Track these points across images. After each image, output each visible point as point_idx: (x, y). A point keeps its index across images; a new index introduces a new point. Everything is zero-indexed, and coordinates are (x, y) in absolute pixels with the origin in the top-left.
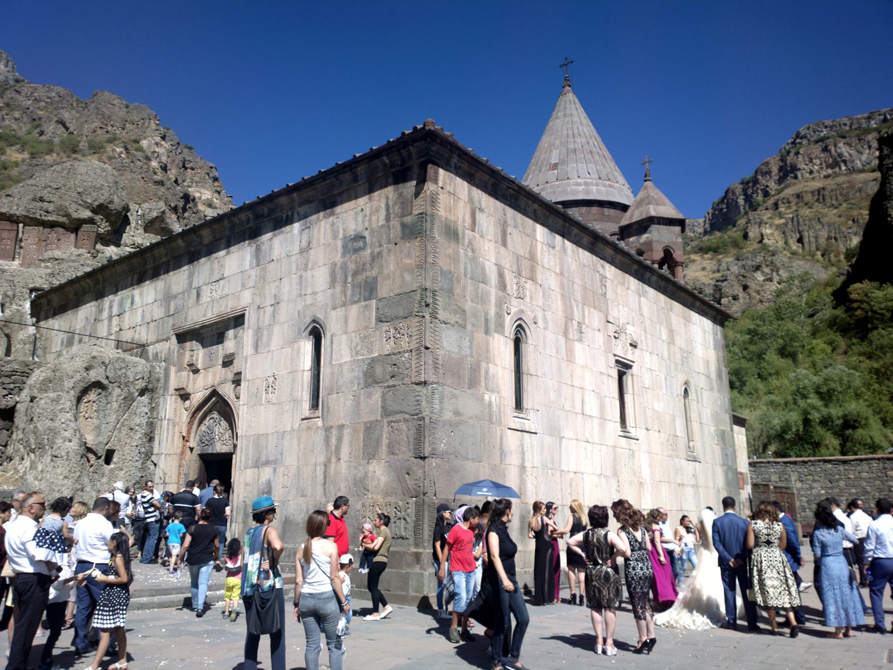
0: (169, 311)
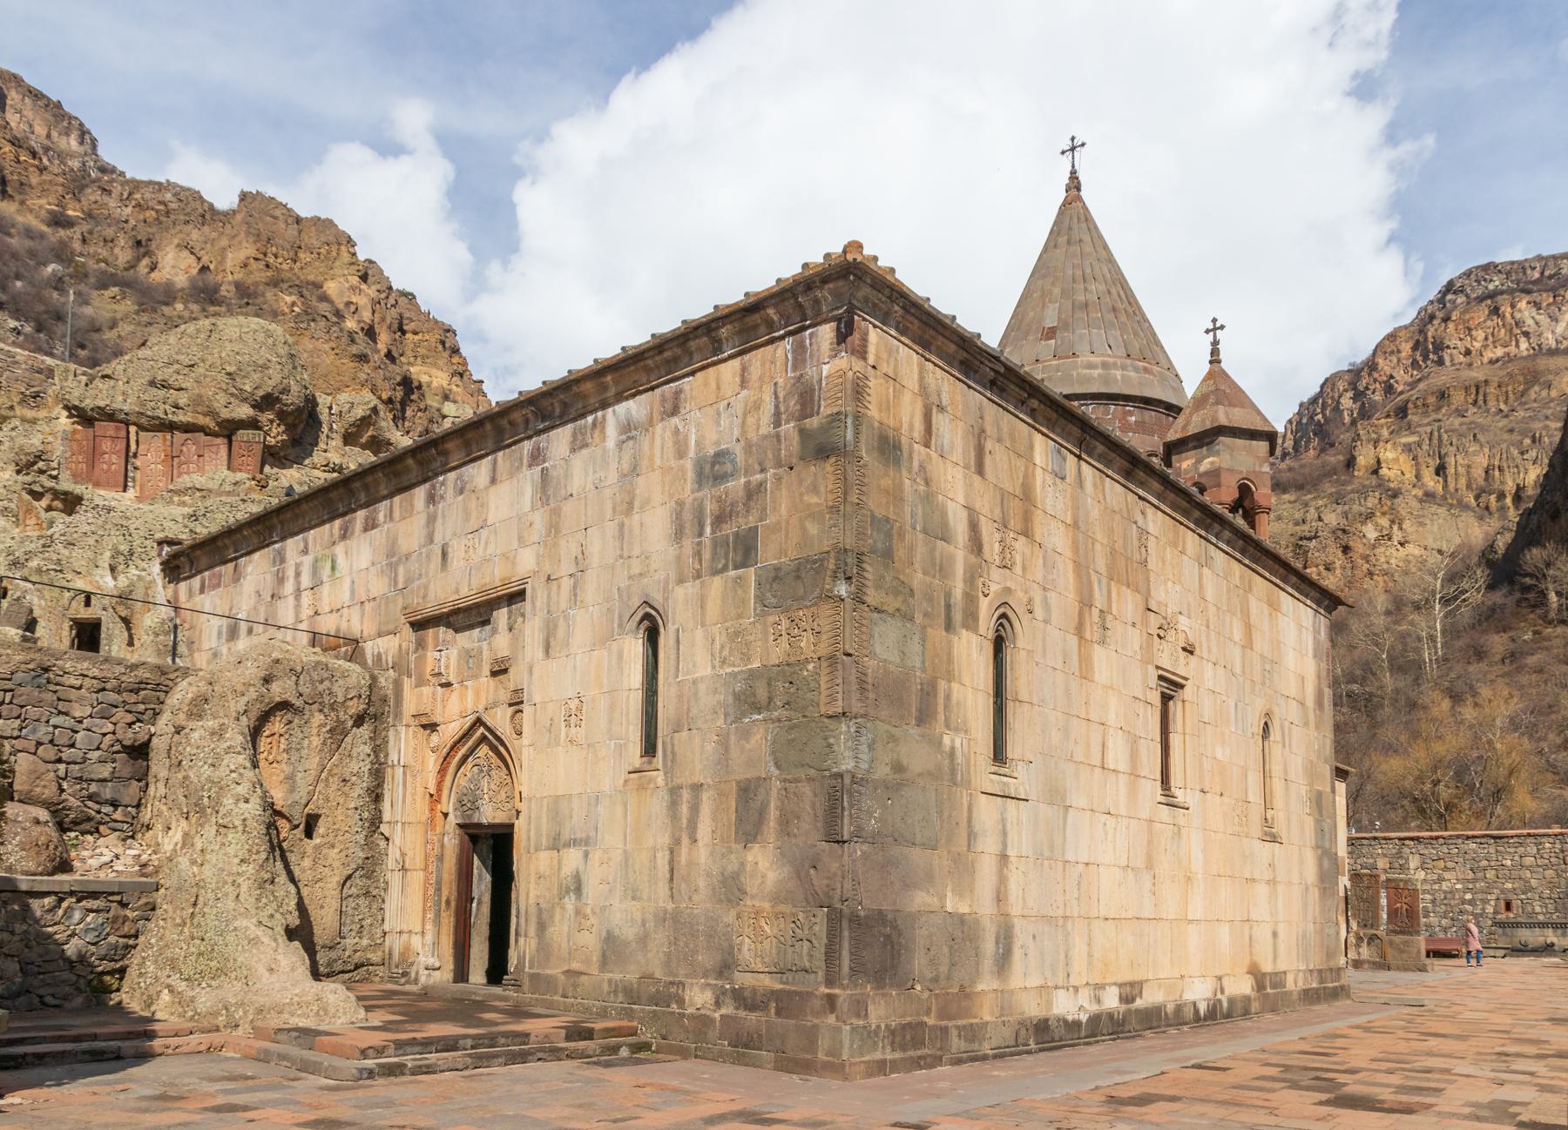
0: (396, 584)
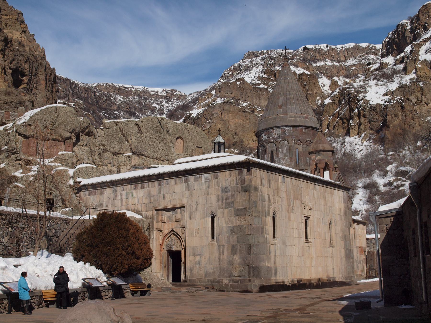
0: (151, 201)
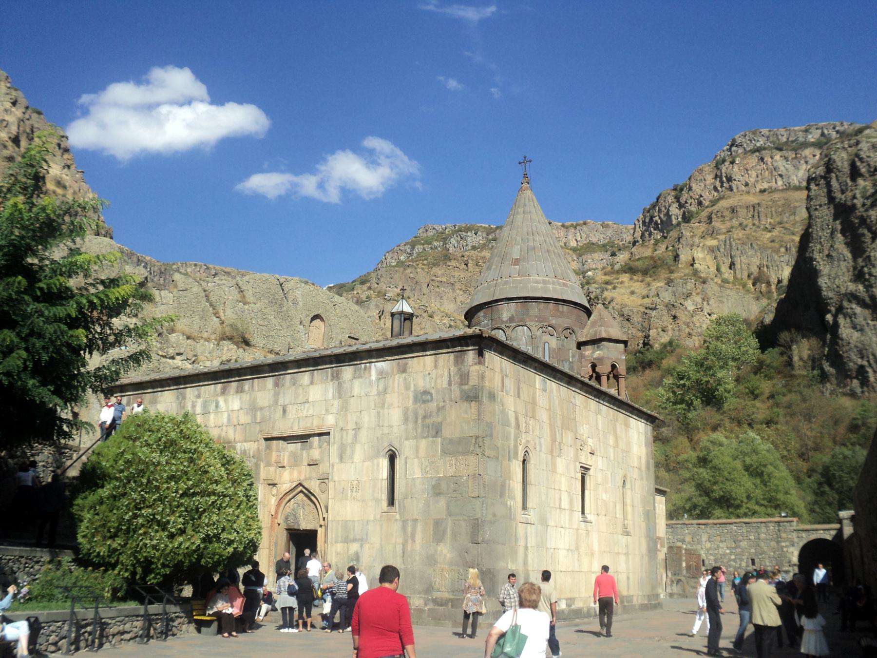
0: (256, 419)
